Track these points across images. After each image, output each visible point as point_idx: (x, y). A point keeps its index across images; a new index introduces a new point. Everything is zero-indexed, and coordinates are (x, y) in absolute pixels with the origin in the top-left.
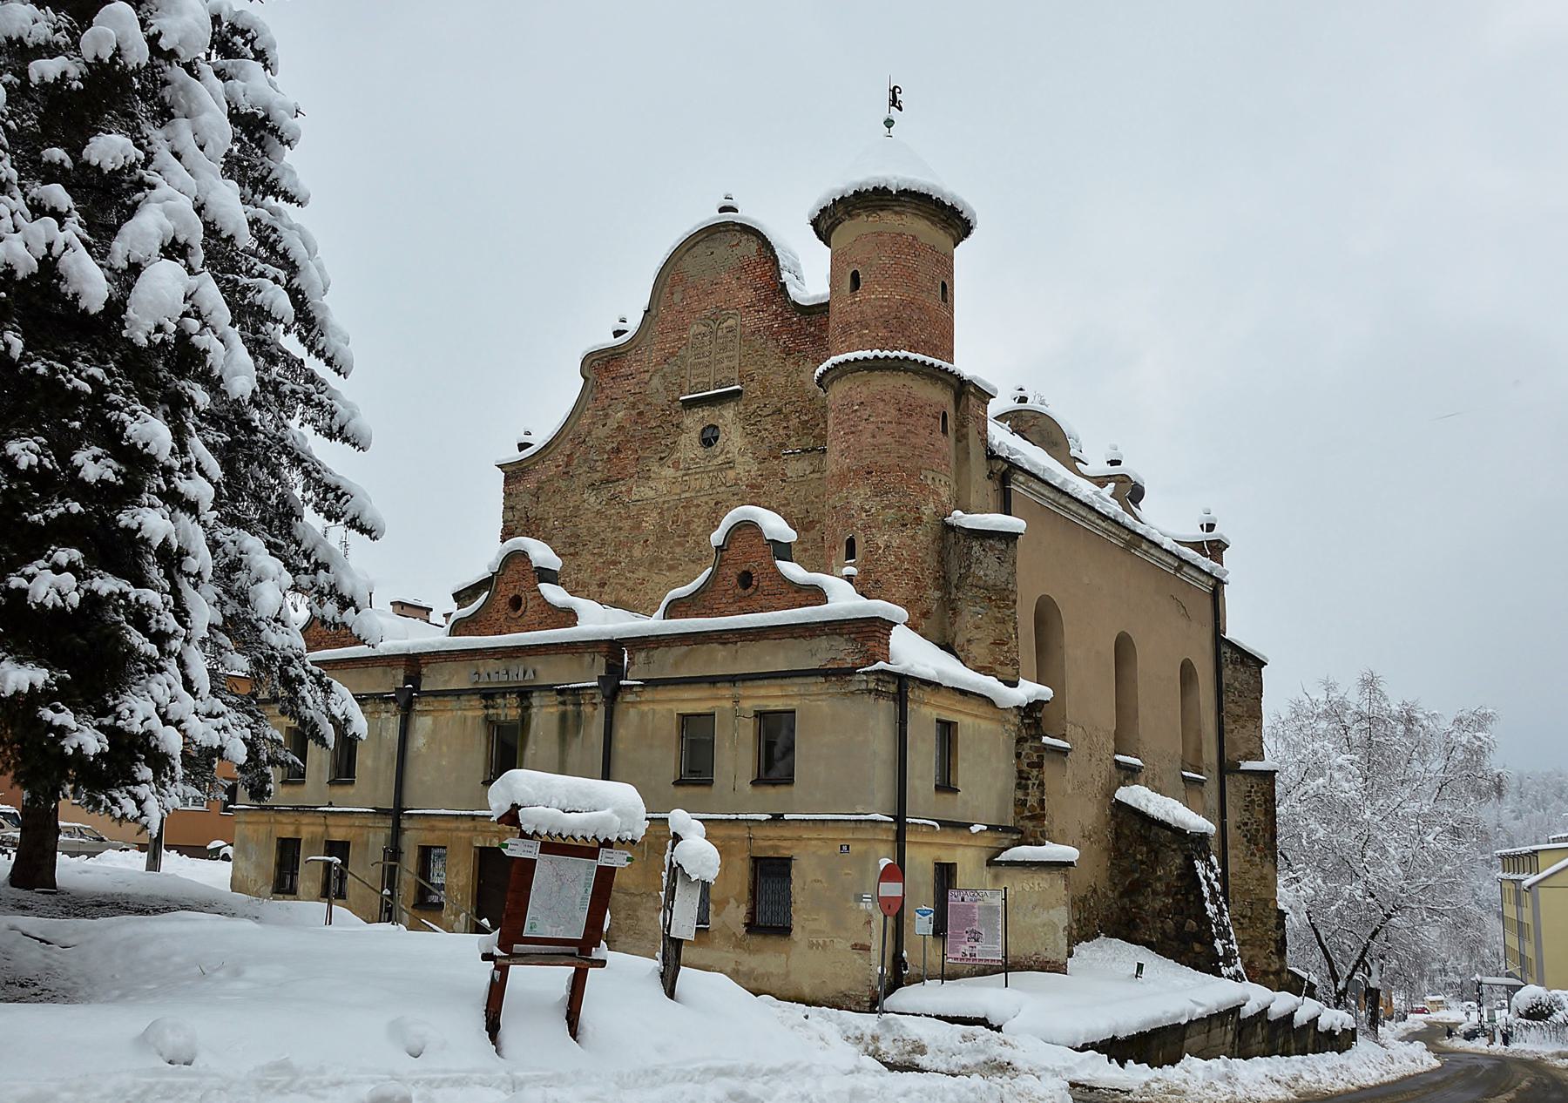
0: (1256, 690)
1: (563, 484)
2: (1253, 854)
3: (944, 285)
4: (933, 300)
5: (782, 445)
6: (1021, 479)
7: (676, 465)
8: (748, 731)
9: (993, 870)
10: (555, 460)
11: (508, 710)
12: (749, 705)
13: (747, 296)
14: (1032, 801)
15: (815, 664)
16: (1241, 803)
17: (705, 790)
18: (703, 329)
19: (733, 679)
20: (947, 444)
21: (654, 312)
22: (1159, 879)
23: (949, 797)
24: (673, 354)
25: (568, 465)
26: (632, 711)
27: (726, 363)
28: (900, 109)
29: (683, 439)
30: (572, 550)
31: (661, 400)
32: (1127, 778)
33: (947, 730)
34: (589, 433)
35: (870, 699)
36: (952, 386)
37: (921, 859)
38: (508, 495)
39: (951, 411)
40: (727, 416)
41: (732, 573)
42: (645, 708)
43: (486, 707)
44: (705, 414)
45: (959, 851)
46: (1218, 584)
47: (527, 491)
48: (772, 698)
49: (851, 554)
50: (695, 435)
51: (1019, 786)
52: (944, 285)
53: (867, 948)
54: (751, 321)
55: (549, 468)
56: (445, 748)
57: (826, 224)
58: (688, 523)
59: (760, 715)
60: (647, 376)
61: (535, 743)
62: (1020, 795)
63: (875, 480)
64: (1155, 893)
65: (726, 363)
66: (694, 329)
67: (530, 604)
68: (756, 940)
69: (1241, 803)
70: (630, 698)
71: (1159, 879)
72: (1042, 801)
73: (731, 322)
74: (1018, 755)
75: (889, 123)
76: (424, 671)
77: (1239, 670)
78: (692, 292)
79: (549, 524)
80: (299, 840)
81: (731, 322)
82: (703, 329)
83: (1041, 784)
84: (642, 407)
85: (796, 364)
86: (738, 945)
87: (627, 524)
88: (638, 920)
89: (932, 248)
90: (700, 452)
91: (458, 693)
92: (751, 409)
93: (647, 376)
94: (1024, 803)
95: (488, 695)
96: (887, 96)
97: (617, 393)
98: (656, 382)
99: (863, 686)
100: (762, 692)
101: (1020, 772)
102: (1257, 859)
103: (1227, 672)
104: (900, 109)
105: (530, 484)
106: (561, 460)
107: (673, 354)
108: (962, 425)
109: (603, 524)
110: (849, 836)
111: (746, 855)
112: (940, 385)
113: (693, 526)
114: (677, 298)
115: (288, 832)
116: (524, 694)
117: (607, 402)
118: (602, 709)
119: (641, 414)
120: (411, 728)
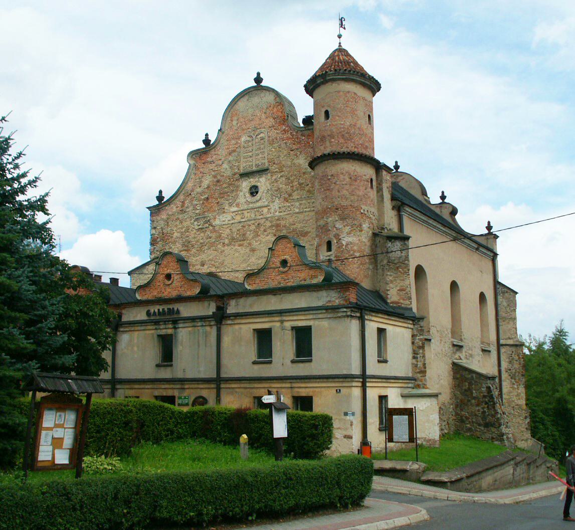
0: (512, 305)
1: (181, 216)
2: (514, 384)
3: (369, 116)
4: (363, 122)
6: (407, 209)
7: (238, 205)
9: (404, 399)
10: (175, 204)
12: (288, 325)
13: (270, 122)
14: (420, 364)
15: (320, 304)
16: (507, 360)
19: (281, 312)
20: (373, 194)
21: (223, 130)
22: (475, 398)
23: (384, 364)
24: (234, 151)
25: (183, 206)
26: (230, 329)
27: (260, 156)
28: (345, 28)
30: (186, 248)
31: (229, 173)
32: (457, 350)
33: (381, 332)
34: (193, 191)
35: (348, 320)
36: (375, 166)
37: (373, 394)
38: (152, 221)
39: (374, 178)
40: (263, 183)
41: (277, 261)
42: (237, 327)
43: (156, 329)
44: (253, 181)
45: (389, 389)
46: (496, 255)
47: (163, 219)
48: (301, 321)
49: (329, 249)
51: (414, 358)
52: (369, 116)
53: (350, 437)
54: (273, 133)
55: (174, 208)
56: (136, 349)
57: (311, 87)
58: (244, 235)
59: (293, 328)
61: (182, 345)
62: (414, 361)
63: (340, 212)
64: (471, 404)
66: (243, 139)
67: (176, 278)
69: (507, 360)
70: (229, 322)
71: (475, 398)
72: (424, 364)
73: (262, 135)
74: (413, 343)
75: (340, 36)
76: (124, 311)
77: (504, 295)
78: (242, 120)
79: (176, 235)
81: (262, 135)
82: (248, 139)
83: (424, 356)
84: (219, 177)
85: (296, 155)
87: (214, 235)
89: (364, 99)
90: (249, 198)
92: (274, 178)
93: (220, 162)
94: (416, 366)
96: (338, 22)
97: (206, 171)
98: (225, 166)
99: (345, 314)
100: (295, 318)
101: (414, 351)
102: (516, 386)
103: (500, 298)
104: (345, 28)
105: (163, 215)
107: (234, 151)
108: (380, 184)
109: (202, 234)
112: (369, 166)
114: (235, 123)
117: (201, 175)
118: (215, 328)
119: (218, 181)
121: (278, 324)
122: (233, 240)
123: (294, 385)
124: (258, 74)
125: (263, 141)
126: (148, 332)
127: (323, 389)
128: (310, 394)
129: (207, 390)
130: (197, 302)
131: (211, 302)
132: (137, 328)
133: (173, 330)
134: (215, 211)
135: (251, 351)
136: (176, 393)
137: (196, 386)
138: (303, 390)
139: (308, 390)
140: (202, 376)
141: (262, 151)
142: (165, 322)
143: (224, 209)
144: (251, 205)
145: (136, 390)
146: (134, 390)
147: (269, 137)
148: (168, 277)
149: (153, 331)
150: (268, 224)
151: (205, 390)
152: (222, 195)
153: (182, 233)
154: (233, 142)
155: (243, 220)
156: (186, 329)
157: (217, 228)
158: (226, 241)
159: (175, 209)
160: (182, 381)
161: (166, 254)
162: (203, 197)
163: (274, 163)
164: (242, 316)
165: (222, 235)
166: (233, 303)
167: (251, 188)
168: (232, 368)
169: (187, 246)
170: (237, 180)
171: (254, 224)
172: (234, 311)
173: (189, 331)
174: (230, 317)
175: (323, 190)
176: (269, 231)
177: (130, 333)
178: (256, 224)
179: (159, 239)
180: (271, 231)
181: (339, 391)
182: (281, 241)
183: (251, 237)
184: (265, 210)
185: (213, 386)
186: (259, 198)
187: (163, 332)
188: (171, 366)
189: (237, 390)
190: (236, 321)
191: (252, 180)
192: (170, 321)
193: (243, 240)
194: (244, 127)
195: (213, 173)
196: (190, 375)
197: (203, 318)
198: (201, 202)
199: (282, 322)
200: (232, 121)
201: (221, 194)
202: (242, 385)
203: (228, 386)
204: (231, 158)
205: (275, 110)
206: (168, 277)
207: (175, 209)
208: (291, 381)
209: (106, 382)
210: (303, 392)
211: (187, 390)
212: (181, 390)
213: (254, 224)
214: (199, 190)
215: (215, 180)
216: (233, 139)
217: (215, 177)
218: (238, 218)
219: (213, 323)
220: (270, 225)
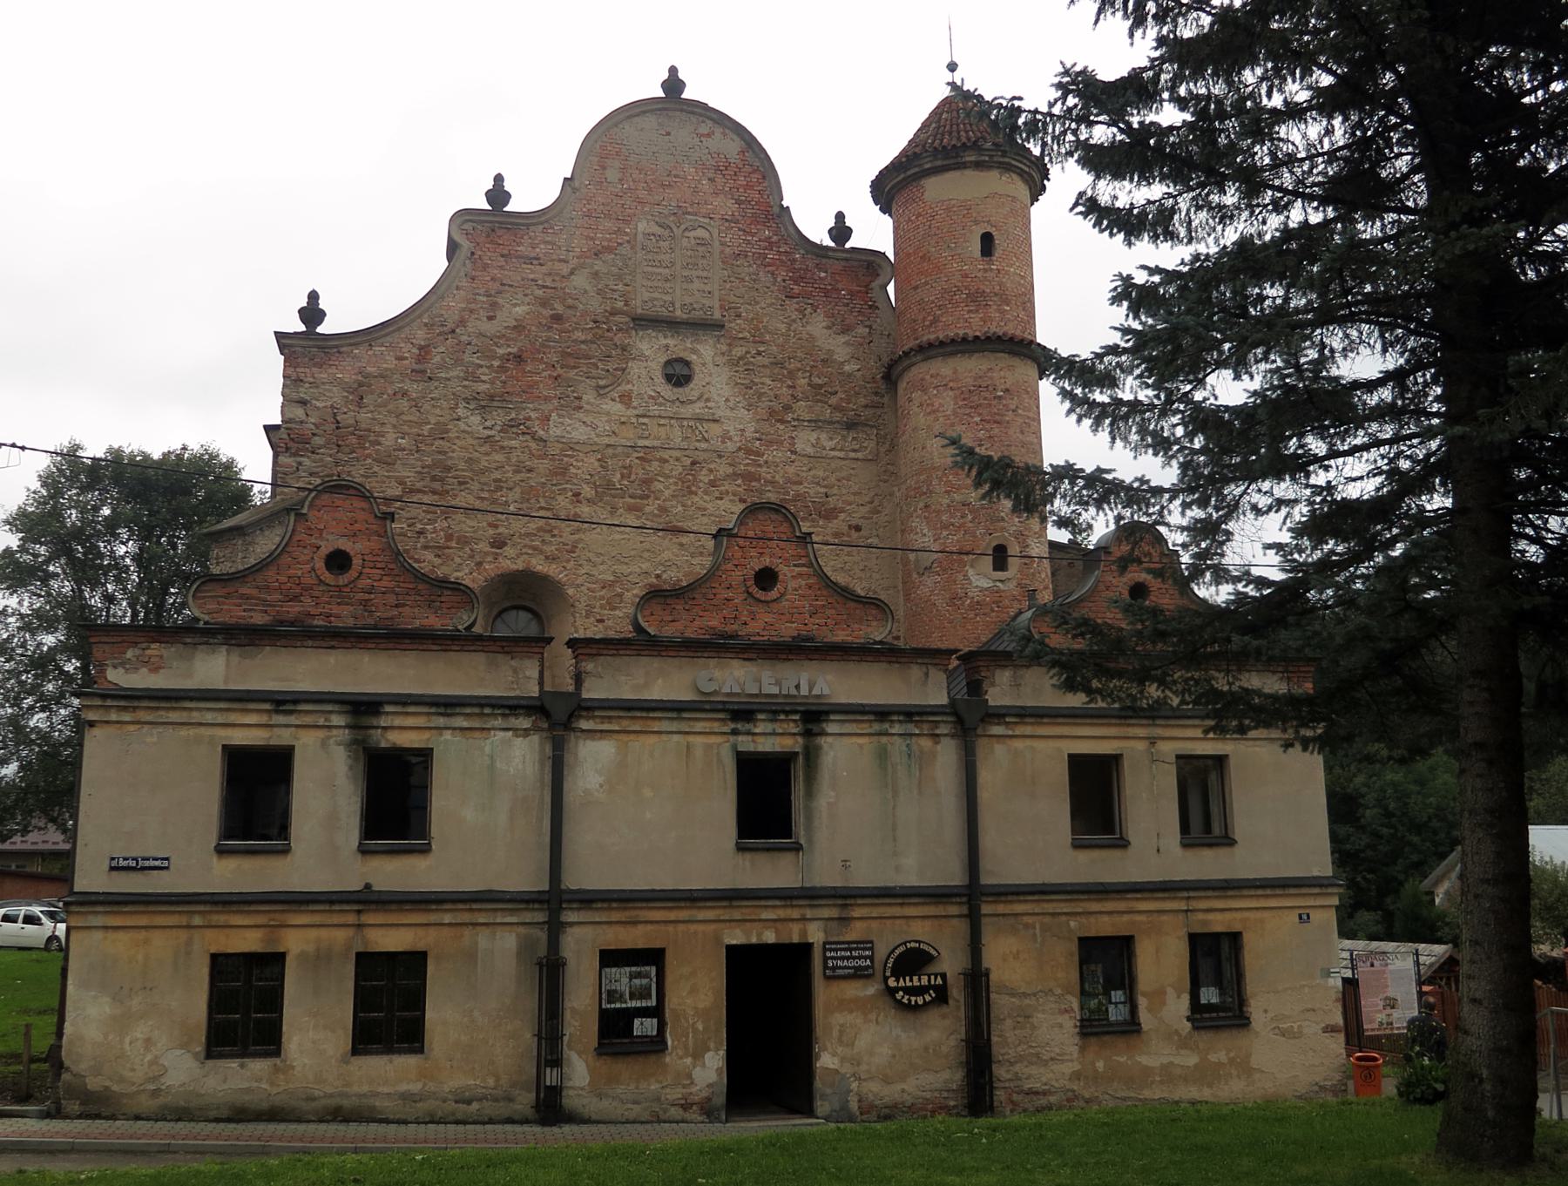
1: (414, 388)
5: (787, 408)
7: (626, 399)
8: (1168, 781)
11: (769, 739)
12: (1169, 749)
13: (726, 206)
17: (1117, 853)
18: (658, 230)
21: (576, 184)
24: (609, 250)
26: (999, 749)
27: (697, 285)
29: (635, 368)
31: (595, 305)
34: (462, 322)
40: (705, 353)
42: (1019, 744)
43: (735, 732)
44: (677, 345)
50: (656, 367)
58: (647, 482)
60: (565, 269)
65: (697, 285)
67: (792, 584)
68: (1205, 1038)
70: (997, 730)
73: (700, 233)
79: (389, 440)
80: (280, 958)
81: (700, 233)
84: (560, 308)
85: (802, 311)
86: (1184, 1044)
88: (1034, 1028)
90: (667, 391)
91: (676, 709)
95: (741, 713)
98: (580, 281)
106: (409, 351)
107: (609, 250)
109: (499, 457)
110: (1311, 902)
111: (1183, 933)
113: (658, 486)
115: (246, 939)
116: (813, 717)
119: (557, 318)
120: (568, 758)
121: (1141, 746)
122: (605, 490)
123: (1195, 904)
124: (673, 70)
125: (701, 249)
126: (699, 740)
127: (1266, 914)
128: (1237, 928)
129: (928, 923)
130: (884, 665)
131: (932, 670)
132: (656, 726)
133: (800, 740)
134: (547, 399)
135: (1054, 809)
136: (816, 935)
137: (897, 911)
138: (1218, 916)
139: (1228, 916)
140: (912, 880)
141: (701, 273)
142: (775, 712)
143: (579, 398)
144: (670, 410)
145: (650, 927)
146: (640, 927)
147: (723, 244)
148: (766, 578)
149: (719, 739)
150: (724, 469)
151: (919, 922)
152: (571, 357)
153: (418, 440)
154: (608, 224)
155: (647, 443)
156: (846, 740)
157: (554, 449)
158: (587, 491)
159: (390, 362)
160: (845, 896)
161: (338, 487)
162: (501, 351)
163: (739, 316)
164: (1042, 716)
165: (573, 470)
166: (1004, 677)
167: (668, 363)
168: (1007, 862)
169: (442, 480)
170: (620, 330)
171: (677, 459)
172: (1007, 701)
173: (861, 746)
174: (1004, 716)
175: (977, 419)
176: (726, 487)
177: (624, 737)
178: (689, 461)
179: (318, 441)
180: (731, 488)
181: (1304, 919)
182: (338, 499)
183: (667, 493)
184: (715, 430)
185: (954, 910)
186: (696, 394)
187: (766, 745)
188: (797, 848)
189: (1026, 919)
190: (1019, 730)
191: (671, 342)
192: (796, 712)
193: (642, 498)
194: (642, 194)
195: (540, 292)
196: (863, 878)
197: (910, 714)
198: (496, 363)
199: (1153, 741)
200: (604, 168)
201: (565, 354)
202: (1049, 907)
203: (1001, 908)
204: (598, 266)
205: (742, 181)
206: (766, 578)
207: (390, 362)
208: (1192, 894)
209: (522, 901)
210: (1219, 923)
211: (859, 925)
212: (834, 924)
213: (677, 459)
214: (490, 328)
215: (547, 312)
216: (608, 216)
217: (544, 303)
218: (627, 436)
219: (943, 729)
220: (730, 470)
